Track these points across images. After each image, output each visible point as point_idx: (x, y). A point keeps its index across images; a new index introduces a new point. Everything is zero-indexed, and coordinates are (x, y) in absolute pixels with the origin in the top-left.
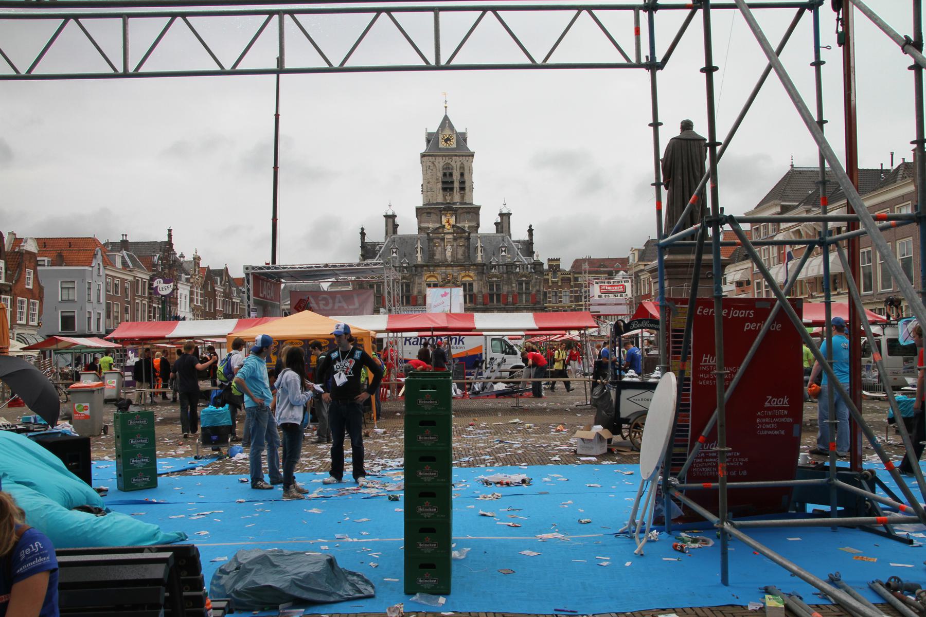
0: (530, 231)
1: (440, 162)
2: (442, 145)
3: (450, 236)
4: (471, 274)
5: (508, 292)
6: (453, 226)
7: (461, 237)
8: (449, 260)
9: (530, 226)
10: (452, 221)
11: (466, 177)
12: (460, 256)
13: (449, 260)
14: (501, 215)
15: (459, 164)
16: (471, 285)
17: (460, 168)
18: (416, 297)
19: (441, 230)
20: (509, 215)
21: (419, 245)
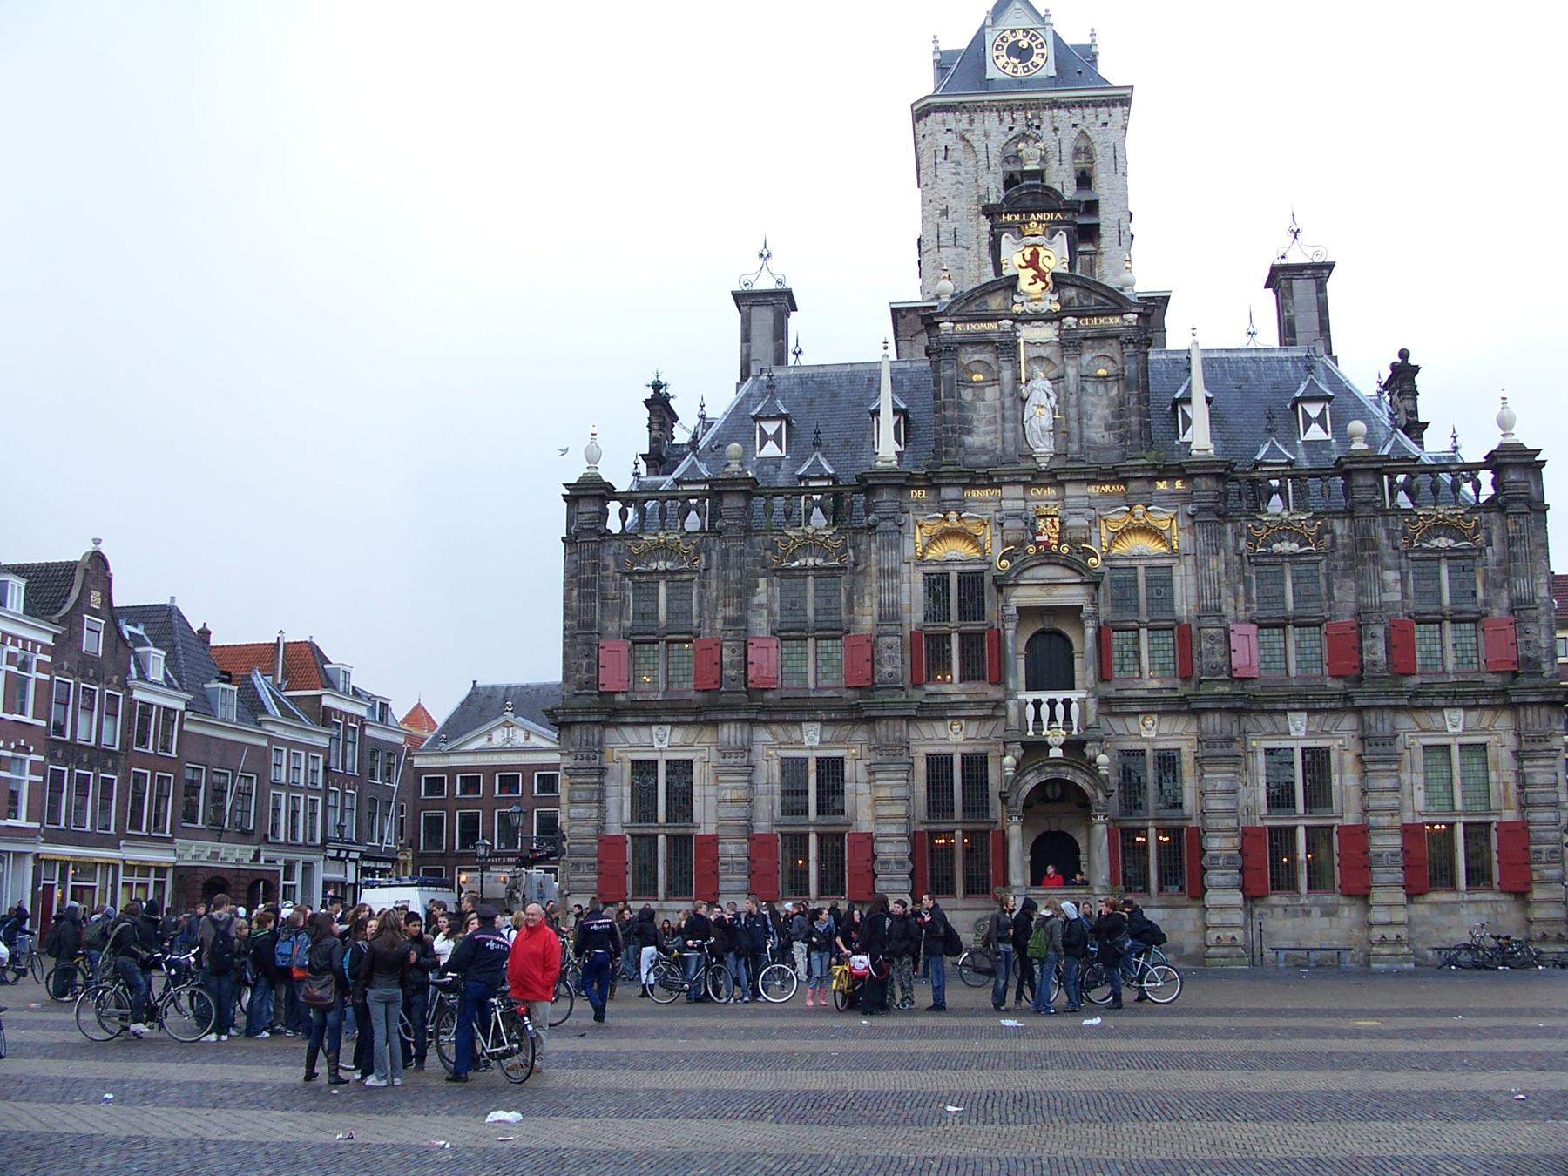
0: (1403, 377)
1: (992, 132)
2: (999, 66)
3: (1047, 332)
4: (1161, 518)
5: (1362, 615)
6: (1059, 282)
7: (1101, 337)
8: (1043, 447)
9: (1404, 354)
10: (1055, 257)
11: (1102, 188)
12: (1097, 432)
13: (1043, 447)
14: (1280, 278)
15: (1069, 139)
16: (1161, 580)
17: (1077, 152)
18: (872, 643)
19: (995, 303)
20: (1320, 272)
21: (886, 401)
